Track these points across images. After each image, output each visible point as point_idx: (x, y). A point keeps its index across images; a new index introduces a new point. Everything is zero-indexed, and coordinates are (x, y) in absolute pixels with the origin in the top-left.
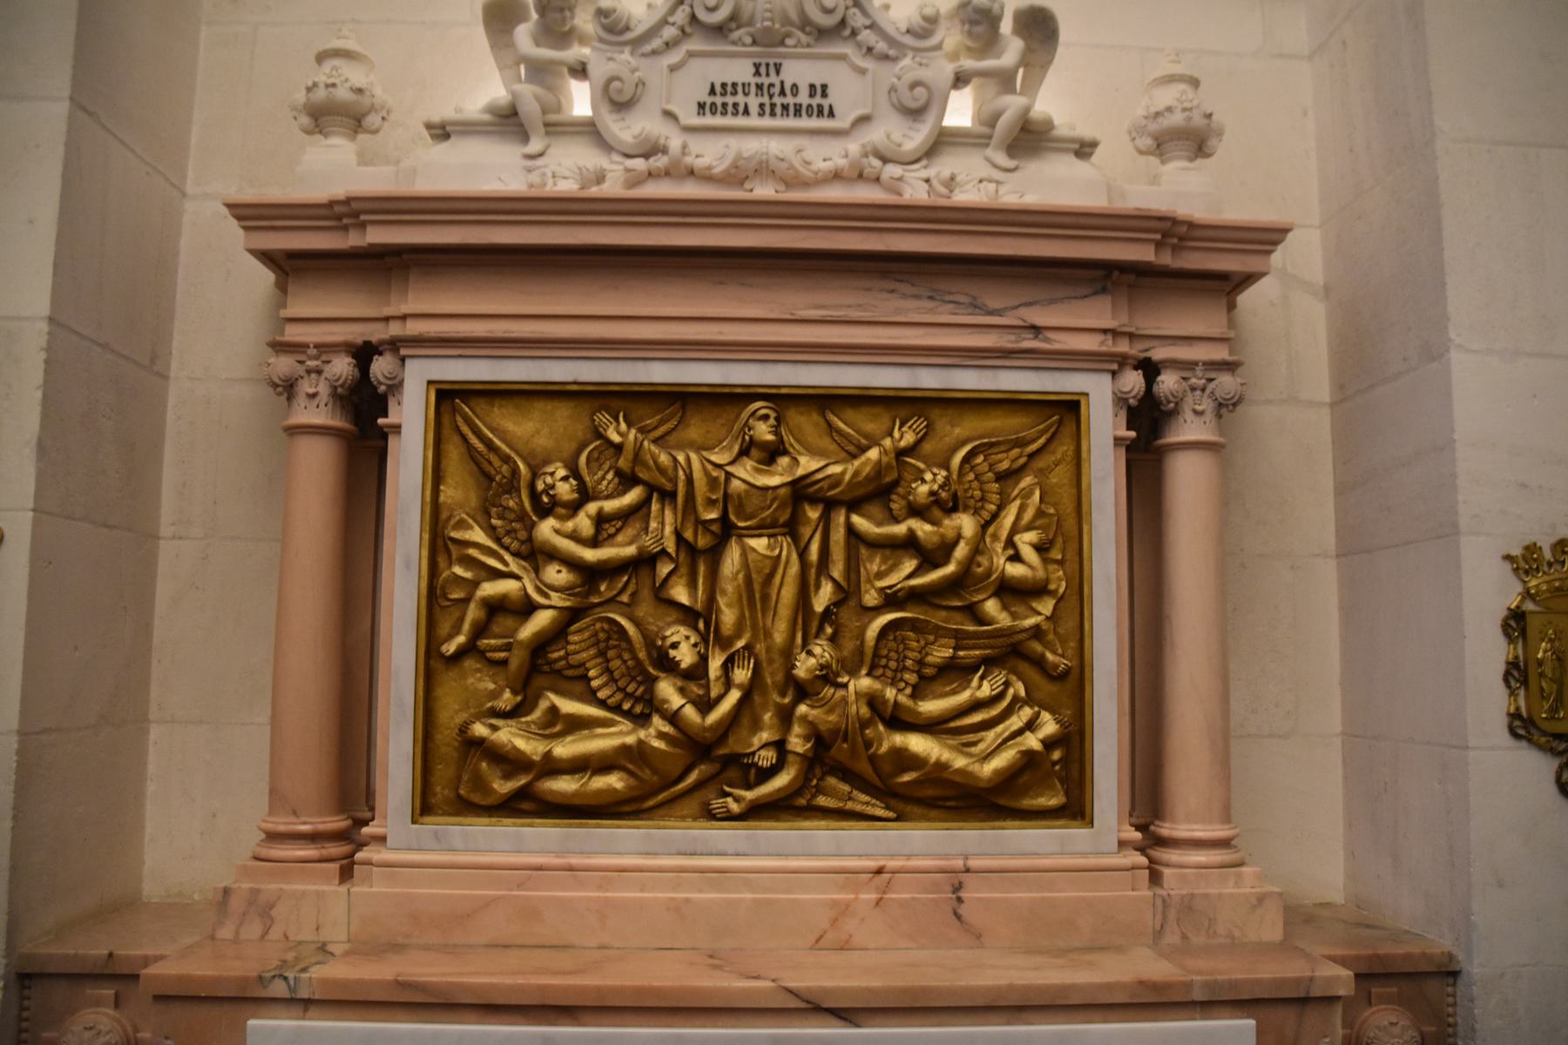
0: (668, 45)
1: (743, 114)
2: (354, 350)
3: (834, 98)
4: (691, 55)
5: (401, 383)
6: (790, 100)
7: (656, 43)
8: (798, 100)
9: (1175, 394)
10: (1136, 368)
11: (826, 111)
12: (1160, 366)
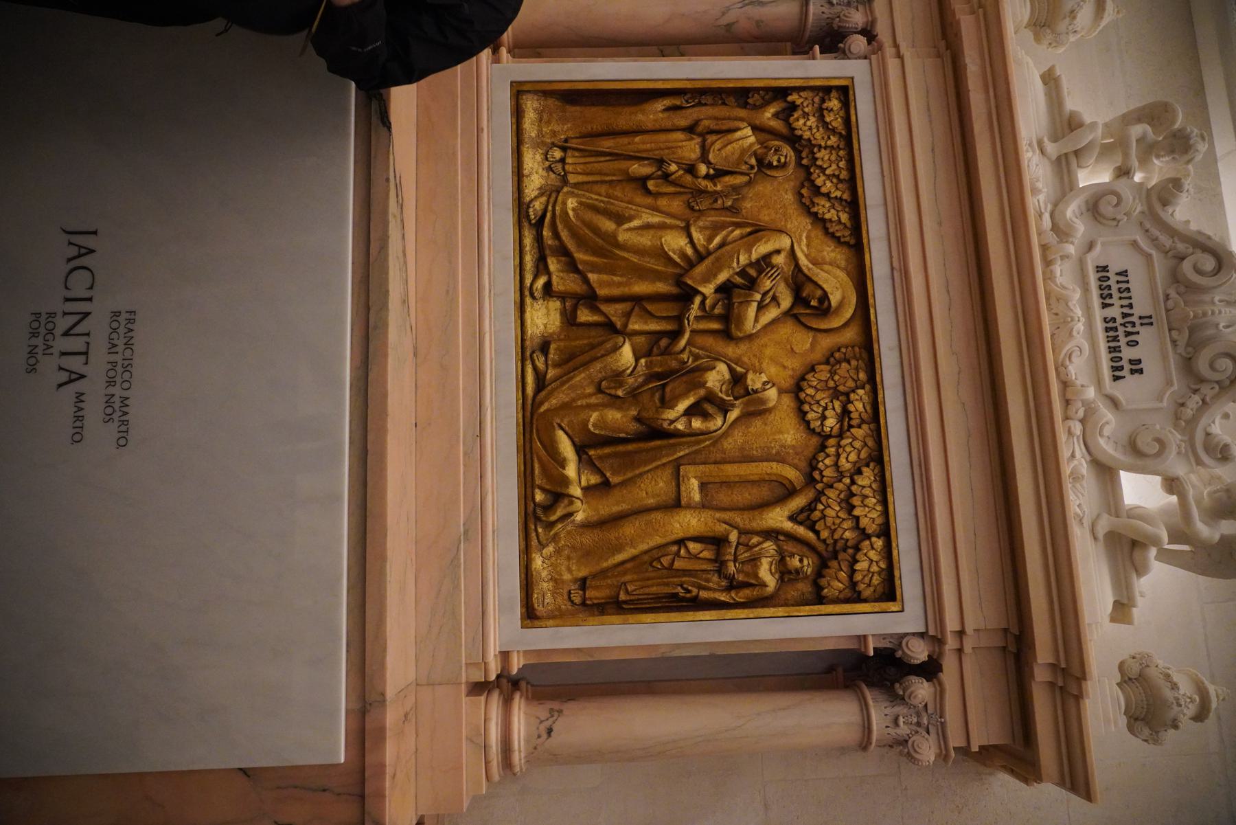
0: (1154, 241)
1: (1103, 303)
2: (869, 28)
3: (1131, 381)
4: (1148, 257)
5: (849, 58)
6: (1123, 340)
7: (1156, 232)
8: (1124, 348)
9: (913, 695)
10: (929, 656)
11: (1117, 373)
12: (935, 680)
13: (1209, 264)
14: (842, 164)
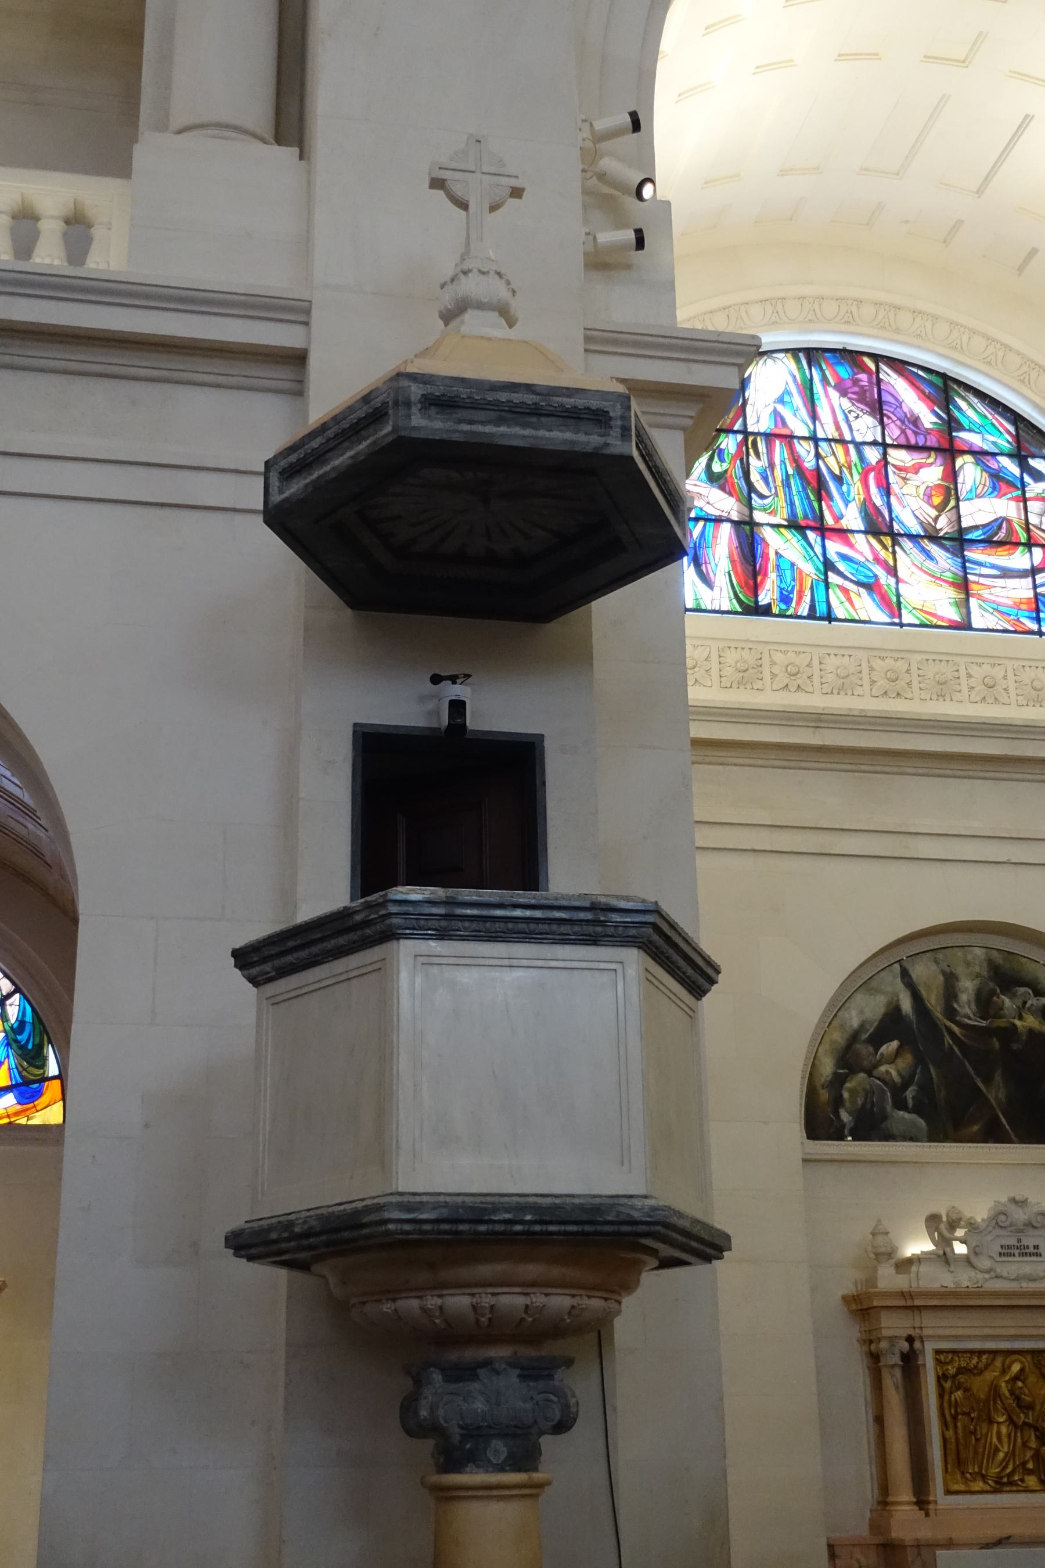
3: (1041, 1250)
4: (998, 1236)
6: (1027, 1251)
13: (1003, 1218)
14: (965, 1355)
